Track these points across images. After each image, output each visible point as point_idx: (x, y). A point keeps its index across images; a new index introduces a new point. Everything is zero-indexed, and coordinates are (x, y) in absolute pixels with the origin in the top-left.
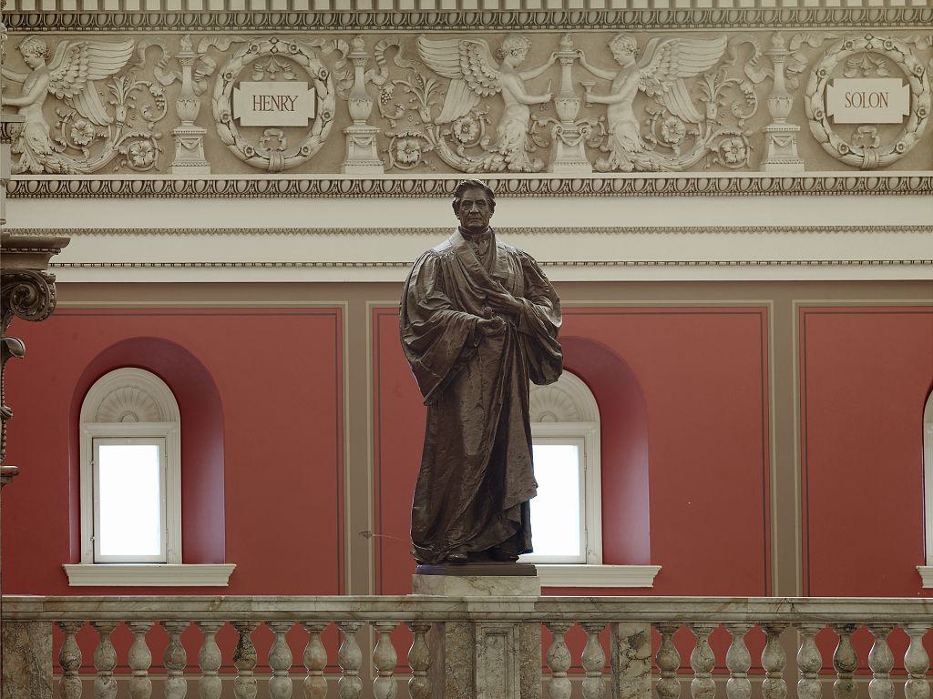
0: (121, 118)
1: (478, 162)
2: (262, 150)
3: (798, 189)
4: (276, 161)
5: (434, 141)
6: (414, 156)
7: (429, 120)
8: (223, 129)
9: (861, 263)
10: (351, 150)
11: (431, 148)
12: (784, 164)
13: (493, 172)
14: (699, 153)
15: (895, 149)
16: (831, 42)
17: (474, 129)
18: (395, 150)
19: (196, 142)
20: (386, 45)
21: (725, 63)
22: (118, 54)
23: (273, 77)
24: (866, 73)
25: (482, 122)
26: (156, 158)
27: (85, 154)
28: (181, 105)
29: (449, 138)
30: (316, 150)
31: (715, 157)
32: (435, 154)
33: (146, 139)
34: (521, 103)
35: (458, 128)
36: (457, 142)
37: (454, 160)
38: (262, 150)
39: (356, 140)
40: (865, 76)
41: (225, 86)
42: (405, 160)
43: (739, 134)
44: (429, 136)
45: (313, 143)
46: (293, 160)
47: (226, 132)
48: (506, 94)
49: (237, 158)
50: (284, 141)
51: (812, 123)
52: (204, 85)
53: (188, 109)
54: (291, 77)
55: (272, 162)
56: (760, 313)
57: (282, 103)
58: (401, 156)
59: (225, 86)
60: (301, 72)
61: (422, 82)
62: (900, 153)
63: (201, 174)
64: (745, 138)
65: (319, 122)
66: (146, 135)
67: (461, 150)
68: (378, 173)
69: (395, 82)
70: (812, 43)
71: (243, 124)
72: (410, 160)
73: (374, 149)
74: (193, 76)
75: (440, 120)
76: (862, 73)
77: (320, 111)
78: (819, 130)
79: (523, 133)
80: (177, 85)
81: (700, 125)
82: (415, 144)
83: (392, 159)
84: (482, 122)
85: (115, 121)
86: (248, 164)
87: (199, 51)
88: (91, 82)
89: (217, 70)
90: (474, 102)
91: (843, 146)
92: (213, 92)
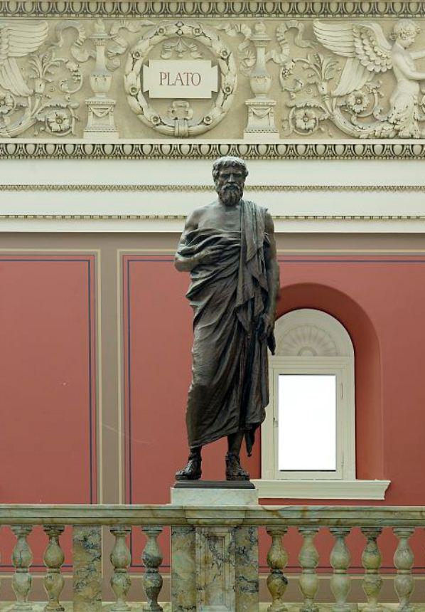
0: (40, 90)
1: (369, 130)
2: (169, 121)
3: (118, 153)
4: (183, 128)
5: (331, 111)
6: (311, 124)
7: (325, 92)
8: (132, 101)
9: (26, 217)
10: (252, 121)
11: (326, 118)
12: (99, 134)
13: (383, 138)
14: (27, 122)
15: (203, 121)
16: (148, 28)
17: (366, 101)
18: (294, 119)
19: (107, 111)
20: (287, 27)
21: (52, 45)
22: (37, 34)
23: (181, 55)
24: (181, 55)
25: (376, 95)
26: (73, 125)
27: (5, 121)
28: (92, 79)
29: (344, 108)
30: (218, 120)
31: (40, 125)
32: (330, 121)
33: (63, 108)
34: (411, 79)
35: (351, 100)
36: (351, 112)
37: (348, 128)
38: (169, 121)
39: (254, 111)
40: (181, 58)
41: (134, 63)
42: (303, 127)
43: (65, 106)
44: (326, 106)
45: (216, 113)
46: (196, 128)
47: (138, 103)
48: (396, 70)
49: (146, 125)
50: (191, 111)
51: (129, 97)
52: (117, 62)
53: (103, 83)
54: (195, 55)
55: (177, 129)
56: (129, 261)
57: (189, 79)
58: (300, 123)
59: (134, 63)
60: (205, 52)
61: (320, 60)
62: (207, 125)
63: (110, 139)
64: (71, 110)
65: (221, 95)
66: (62, 105)
67: (354, 119)
68: (274, 139)
69: (295, 60)
70: (131, 28)
71: (151, 96)
72: (307, 127)
73: (272, 119)
74: (106, 55)
75: (335, 93)
76: (177, 55)
77: (223, 86)
78: (138, 103)
79: (411, 105)
80: (91, 62)
81: (29, 98)
82: (312, 113)
83: (292, 126)
84: (376, 95)
85: (34, 92)
86: (155, 131)
87: (111, 33)
88: (14, 59)
89: (128, 48)
90: (368, 78)
91: (155, 117)
92: (124, 67)
